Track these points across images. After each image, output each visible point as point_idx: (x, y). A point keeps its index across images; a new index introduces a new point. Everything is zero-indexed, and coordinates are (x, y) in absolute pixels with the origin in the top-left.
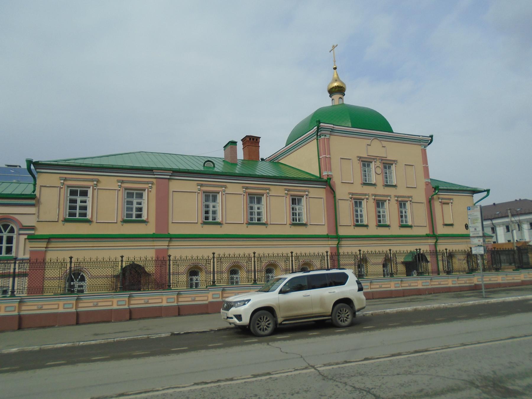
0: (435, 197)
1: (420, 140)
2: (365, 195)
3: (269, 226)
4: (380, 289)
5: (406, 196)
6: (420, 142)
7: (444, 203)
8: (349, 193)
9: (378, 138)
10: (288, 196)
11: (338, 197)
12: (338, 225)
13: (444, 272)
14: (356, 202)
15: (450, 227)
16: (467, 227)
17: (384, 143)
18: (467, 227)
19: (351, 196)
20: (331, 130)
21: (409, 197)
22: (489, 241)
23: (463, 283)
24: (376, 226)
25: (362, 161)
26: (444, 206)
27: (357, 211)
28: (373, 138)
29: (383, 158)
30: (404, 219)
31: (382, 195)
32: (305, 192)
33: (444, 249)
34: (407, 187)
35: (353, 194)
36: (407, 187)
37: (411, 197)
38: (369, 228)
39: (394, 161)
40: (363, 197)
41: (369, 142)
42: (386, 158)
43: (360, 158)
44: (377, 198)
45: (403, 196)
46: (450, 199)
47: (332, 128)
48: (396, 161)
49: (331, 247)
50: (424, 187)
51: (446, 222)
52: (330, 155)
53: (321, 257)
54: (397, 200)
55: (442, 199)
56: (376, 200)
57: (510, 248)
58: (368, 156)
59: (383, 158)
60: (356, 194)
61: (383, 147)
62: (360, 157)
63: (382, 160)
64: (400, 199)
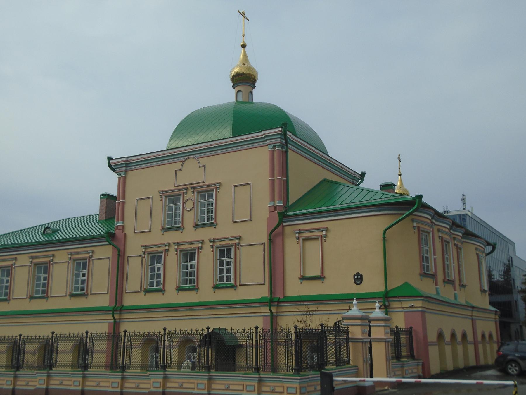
0: (288, 230)
1: (265, 137)
2: (163, 245)
3: (50, 300)
4: (61, 386)
5: (228, 238)
6: (267, 140)
7: (304, 240)
8: (142, 246)
9: (194, 156)
10: (72, 261)
11: (128, 253)
12: (124, 292)
13: (79, 366)
14: (153, 258)
15: (318, 283)
16: (358, 279)
17: (203, 161)
18: (358, 279)
19: (144, 250)
20: (124, 165)
21: (234, 238)
22: (412, 307)
23: (94, 386)
24: (177, 290)
25: (166, 197)
26: (308, 244)
27: (152, 269)
28: (186, 157)
29: (195, 185)
30: (225, 275)
31: (189, 242)
32: (89, 253)
33: (84, 332)
34: (234, 222)
35: (146, 247)
36: (234, 222)
37: (240, 238)
38: (165, 294)
39: (214, 184)
40: (160, 249)
41: (178, 166)
42: (204, 182)
43: (162, 193)
44: (182, 247)
45: (225, 238)
46: (319, 230)
47: (125, 162)
48: (220, 184)
49: (109, 323)
50: (267, 215)
51: (308, 274)
52: (124, 200)
53: (199, 335)
54: (212, 247)
55: (300, 232)
56: (181, 251)
57: (183, 329)
58: (175, 187)
59: (195, 185)
60: (152, 246)
61: (200, 167)
62: (163, 192)
63: (194, 188)
64: (217, 244)
